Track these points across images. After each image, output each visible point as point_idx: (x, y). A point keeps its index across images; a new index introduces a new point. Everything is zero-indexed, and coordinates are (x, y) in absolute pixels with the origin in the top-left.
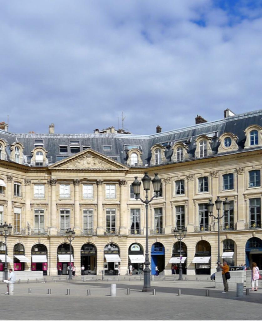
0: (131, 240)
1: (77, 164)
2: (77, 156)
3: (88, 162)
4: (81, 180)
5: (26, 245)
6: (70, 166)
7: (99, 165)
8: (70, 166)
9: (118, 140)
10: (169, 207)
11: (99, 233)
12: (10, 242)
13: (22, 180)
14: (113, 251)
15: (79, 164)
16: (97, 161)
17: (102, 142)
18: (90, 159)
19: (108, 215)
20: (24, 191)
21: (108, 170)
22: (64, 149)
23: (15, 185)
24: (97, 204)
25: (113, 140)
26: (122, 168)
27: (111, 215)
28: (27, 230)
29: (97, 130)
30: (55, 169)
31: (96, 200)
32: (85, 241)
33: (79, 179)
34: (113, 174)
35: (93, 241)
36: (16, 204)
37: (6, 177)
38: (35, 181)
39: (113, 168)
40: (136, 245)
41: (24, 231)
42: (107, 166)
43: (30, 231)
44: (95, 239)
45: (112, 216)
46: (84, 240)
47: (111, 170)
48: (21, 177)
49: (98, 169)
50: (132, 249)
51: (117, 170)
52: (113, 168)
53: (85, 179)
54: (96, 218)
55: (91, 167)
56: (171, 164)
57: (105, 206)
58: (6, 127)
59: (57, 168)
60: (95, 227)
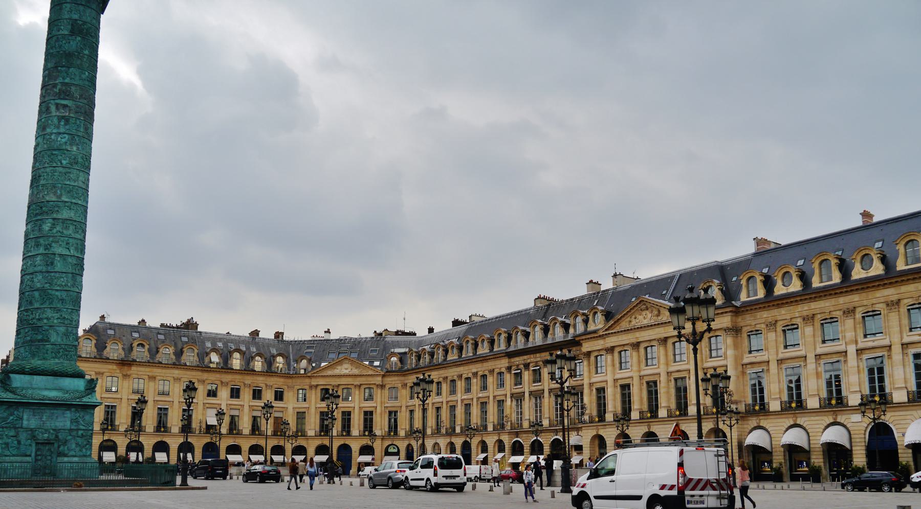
0: (387, 442)
6: (329, 373)
8: (329, 373)
9: (388, 343)
10: (417, 409)
13: (284, 386)
15: (338, 371)
17: (371, 346)
19: (366, 417)
27: (369, 417)
40: (397, 449)
45: (348, 418)
50: (390, 450)
55: (347, 372)
56: (419, 368)
59: (315, 375)
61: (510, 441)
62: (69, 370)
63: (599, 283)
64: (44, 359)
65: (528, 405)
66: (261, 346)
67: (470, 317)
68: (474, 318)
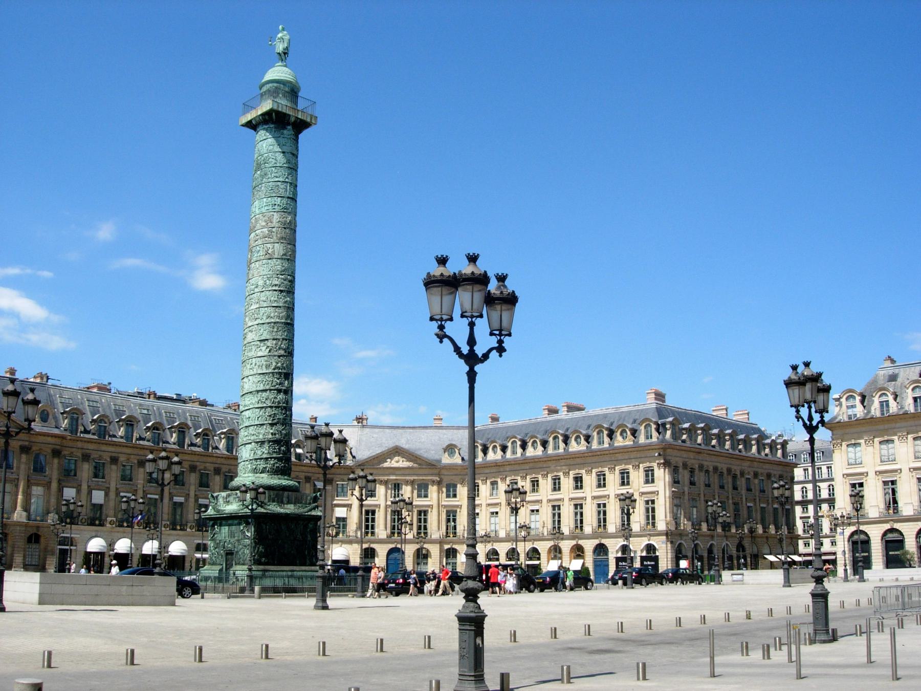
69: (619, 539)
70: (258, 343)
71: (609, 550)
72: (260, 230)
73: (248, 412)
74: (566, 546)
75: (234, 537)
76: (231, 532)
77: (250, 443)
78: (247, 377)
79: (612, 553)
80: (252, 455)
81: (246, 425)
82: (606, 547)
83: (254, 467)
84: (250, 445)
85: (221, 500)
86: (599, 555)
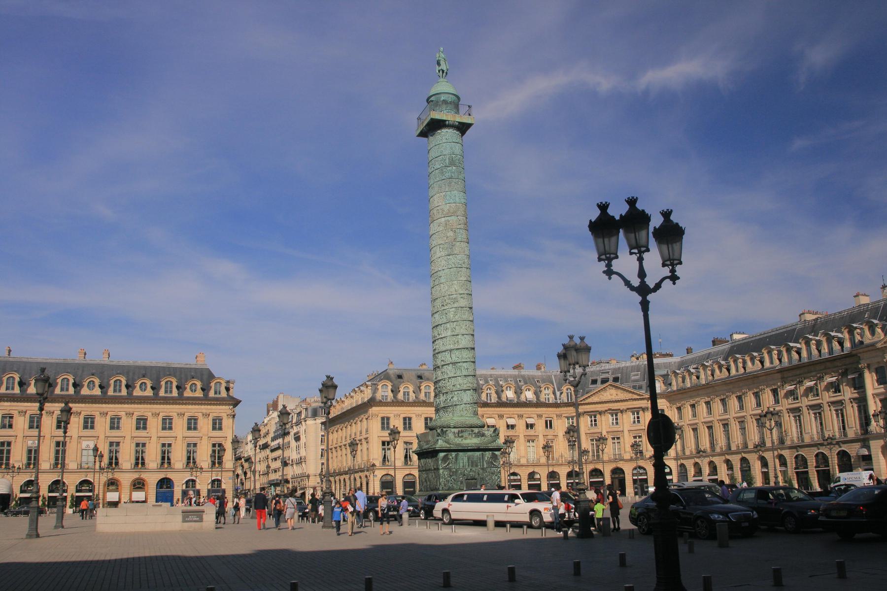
1: (601, 396)
2: (605, 386)
3: (611, 394)
4: (606, 411)
5: (561, 472)
7: (622, 395)
11: (625, 458)
12: (544, 470)
13: (553, 415)
14: (641, 474)
16: (619, 392)
17: (632, 370)
18: (613, 391)
20: (556, 424)
21: (629, 399)
22: (594, 382)
23: (546, 422)
24: (623, 431)
25: (643, 366)
26: (643, 396)
28: (560, 459)
29: (633, 356)
30: (581, 404)
31: (622, 427)
32: (613, 466)
33: (603, 409)
34: (635, 402)
35: (621, 465)
36: (548, 437)
37: (536, 415)
38: (566, 415)
39: (636, 397)
41: (558, 460)
42: (629, 396)
43: (563, 459)
44: (623, 463)
46: (612, 465)
47: (632, 399)
48: (553, 413)
49: (620, 400)
51: (637, 399)
52: (636, 397)
53: (610, 409)
54: (623, 444)
55: (614, 398)
57: (631, 432)
58: (543, 367)
59: (582, 402)
60: (622, 452)
61: (791, 455)
62: (479, 422)
63: (866, 294)
64: (462, 416)
65: (809, 418)
66: (527, 379)
67: (731, 335)
68: (737, 337)
69: (186, 475)
70: (468, 309)
71: (175, 484)
72: (461, 217)
73: (465, 364)
74: (126, 479)
75: (477, 466)
76: (472, 462)
77: (470, 390)
78: (463, 335)
79: (178, 486)
80: (472, 400)
81: (465, 374)
82: (172, 481)
83: (474, 409)
84: (469, 391)
85: (450, 436)
86: (161, 488)
